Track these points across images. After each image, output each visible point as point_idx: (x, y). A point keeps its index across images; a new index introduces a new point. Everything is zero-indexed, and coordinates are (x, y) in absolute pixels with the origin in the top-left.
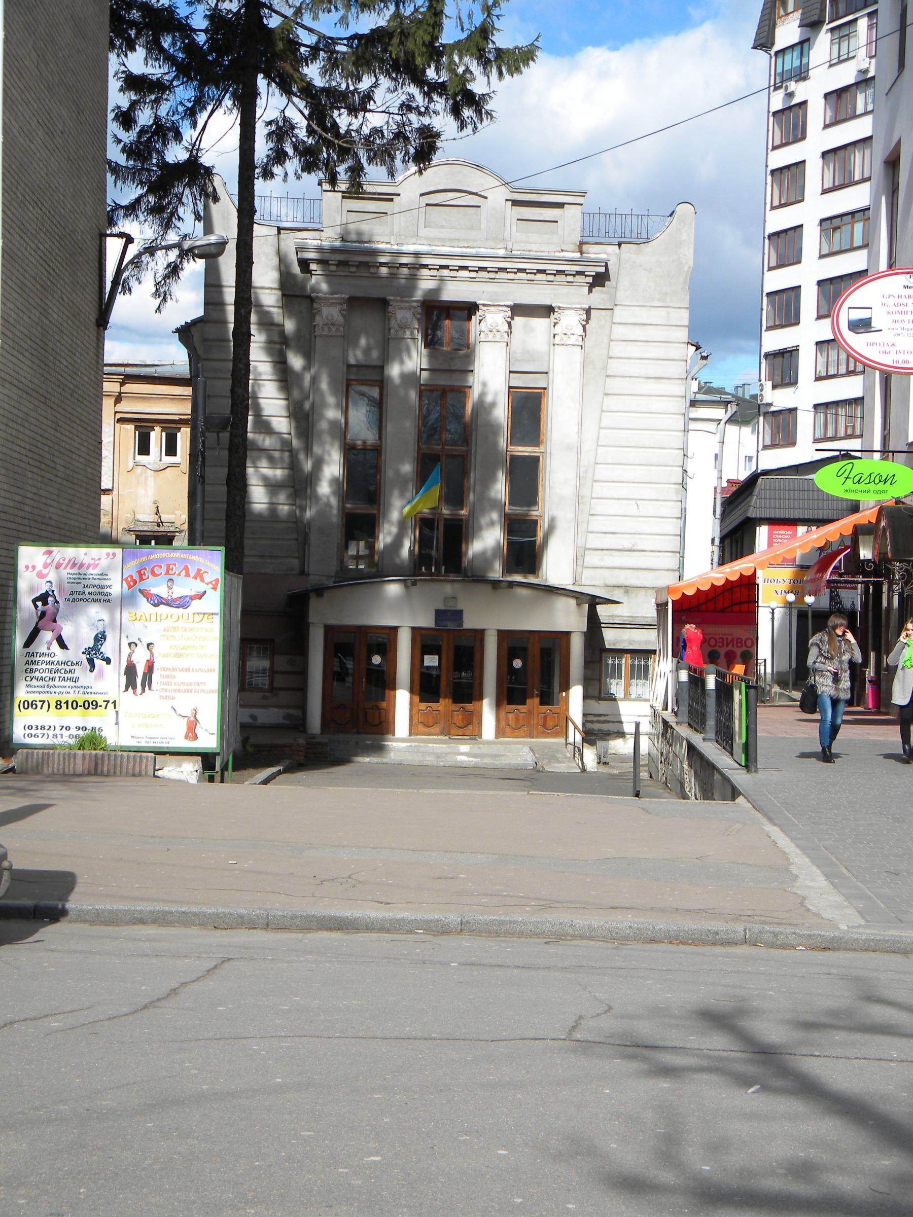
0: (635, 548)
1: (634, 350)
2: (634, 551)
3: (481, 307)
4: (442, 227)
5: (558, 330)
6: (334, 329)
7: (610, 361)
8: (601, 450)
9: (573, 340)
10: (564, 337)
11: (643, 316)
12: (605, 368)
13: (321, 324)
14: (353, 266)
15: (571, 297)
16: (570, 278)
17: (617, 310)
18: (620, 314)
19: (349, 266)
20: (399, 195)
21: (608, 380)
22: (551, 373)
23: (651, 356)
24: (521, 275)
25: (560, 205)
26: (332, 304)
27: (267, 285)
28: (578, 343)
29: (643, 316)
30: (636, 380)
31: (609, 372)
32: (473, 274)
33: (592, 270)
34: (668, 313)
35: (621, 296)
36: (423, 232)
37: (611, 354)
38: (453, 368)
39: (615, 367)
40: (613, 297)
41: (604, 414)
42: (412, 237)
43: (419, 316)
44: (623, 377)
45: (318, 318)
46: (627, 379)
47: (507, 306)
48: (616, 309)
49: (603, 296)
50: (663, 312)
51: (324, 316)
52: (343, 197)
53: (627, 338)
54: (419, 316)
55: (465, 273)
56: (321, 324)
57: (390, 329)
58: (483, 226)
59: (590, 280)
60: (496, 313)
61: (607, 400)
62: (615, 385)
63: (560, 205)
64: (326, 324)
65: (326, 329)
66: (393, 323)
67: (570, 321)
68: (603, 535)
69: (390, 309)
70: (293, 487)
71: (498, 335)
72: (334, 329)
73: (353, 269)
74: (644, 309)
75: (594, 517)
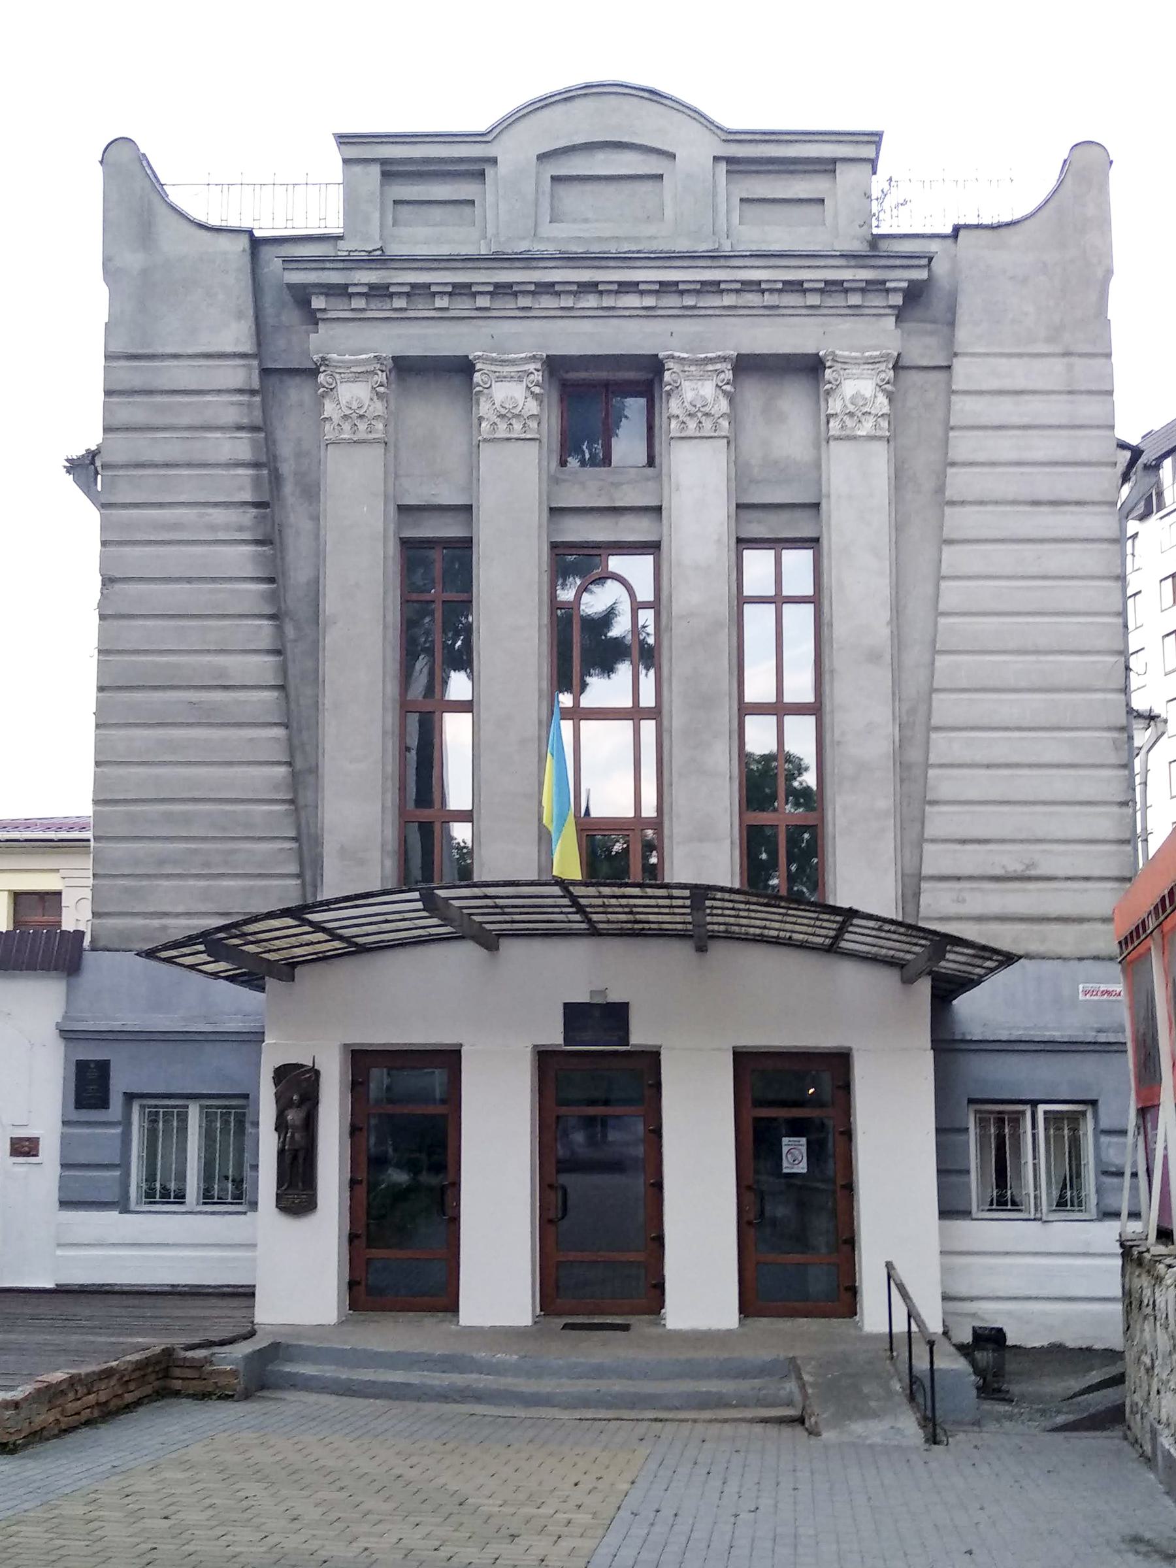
0: (1033, 873)
1: (1004, 447)
2: (1029, 879)
3: (669, 364)
4: (586, 220)
6: (362, 426)
7: (951, 471)
8: (941, 661)
11: (1017, 374)
12: (940, 489)
13: (336, 418)
14: (400, 294)
18: (965, 372)
19: (391, 296)
20: (494, 161)
21: (948, 510)
22: (824, 506)
23: (1039, 455)
24: (753, 299)
25: (828, 167)
26: (358, 377)
27: (229, 349)
28: (879, 433)
29: (1017, 374)
30: (1008, 508)
31: (949, 494)
32: (650, 301)
34: (1070, 368)
35: (962, 334)
36: (547, 229)
37: (953, 455)
38: (617, 504)
39: (959, 482)
40: (950, 340)
41: (944, 584)
42: (524, 238)
43: (537, 390)
44: (982, 503)
46: (990, 508)
48: (959, 365)
49: (932, 341)
50: (1059, 365)
51: (343, 402)
52: (385, 174)
53: (984, 421)
54: (537, 390)
56: (336, 418)
57: (480, 419)
58: (669, 213)
60: (701, 378)
61: (947, 551)
62: (960, 521)
63: (828, 167)
64: (346, 417)
65: (347, 426)
66: (484, 408)
67: (858, 388)
68: (958, 847)
69: (477, 377)
70: (289, 764)
72: (362, 426)
74: (1014, 361)
75: (936, 809)
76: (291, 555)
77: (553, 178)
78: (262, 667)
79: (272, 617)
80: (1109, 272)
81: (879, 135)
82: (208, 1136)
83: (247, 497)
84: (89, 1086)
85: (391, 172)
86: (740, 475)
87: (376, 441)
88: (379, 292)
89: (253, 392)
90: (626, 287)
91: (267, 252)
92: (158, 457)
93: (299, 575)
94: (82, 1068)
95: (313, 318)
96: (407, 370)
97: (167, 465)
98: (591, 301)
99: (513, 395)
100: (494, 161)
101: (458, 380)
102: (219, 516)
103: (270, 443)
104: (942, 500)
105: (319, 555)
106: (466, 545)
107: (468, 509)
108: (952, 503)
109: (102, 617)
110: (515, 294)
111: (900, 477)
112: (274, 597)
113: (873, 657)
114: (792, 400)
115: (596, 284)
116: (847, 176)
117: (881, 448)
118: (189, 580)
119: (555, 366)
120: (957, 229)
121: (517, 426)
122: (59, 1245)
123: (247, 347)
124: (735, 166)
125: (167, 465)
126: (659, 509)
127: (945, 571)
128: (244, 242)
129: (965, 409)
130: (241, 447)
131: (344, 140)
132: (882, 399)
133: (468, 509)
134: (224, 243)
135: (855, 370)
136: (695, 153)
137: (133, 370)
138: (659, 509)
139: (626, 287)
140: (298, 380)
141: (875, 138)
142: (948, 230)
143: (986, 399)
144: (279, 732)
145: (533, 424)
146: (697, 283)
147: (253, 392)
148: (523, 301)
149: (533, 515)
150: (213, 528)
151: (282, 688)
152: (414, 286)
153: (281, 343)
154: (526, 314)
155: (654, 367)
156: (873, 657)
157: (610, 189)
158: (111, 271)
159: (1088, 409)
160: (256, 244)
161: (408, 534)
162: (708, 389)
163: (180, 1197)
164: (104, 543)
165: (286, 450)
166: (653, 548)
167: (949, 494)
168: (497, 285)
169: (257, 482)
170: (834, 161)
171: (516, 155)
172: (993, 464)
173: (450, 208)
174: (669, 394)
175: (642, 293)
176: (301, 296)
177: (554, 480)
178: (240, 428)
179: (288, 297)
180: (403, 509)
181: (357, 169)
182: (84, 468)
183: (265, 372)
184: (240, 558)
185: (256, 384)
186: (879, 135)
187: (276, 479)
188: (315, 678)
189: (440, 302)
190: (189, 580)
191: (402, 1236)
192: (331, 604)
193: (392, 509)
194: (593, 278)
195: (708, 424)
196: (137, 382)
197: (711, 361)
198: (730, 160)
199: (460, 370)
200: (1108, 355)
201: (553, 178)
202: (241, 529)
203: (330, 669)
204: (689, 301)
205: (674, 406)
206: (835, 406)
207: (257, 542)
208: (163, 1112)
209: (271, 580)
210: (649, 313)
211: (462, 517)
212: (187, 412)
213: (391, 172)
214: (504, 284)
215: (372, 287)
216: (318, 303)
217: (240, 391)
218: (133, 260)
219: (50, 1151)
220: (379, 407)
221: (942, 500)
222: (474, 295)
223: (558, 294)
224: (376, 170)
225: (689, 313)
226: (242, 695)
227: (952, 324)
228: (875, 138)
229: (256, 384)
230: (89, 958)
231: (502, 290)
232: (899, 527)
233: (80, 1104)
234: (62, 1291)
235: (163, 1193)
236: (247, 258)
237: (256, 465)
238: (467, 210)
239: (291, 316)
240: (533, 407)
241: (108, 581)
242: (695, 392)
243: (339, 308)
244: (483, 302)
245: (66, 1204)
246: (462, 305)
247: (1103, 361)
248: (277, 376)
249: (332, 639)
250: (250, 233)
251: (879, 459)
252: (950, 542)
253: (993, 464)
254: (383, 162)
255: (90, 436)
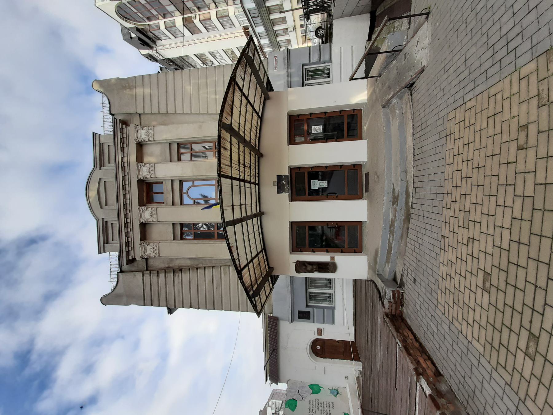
5: (147, 139)
6: (155, 248)
9: (151, 131)
10: (150, 135)
15: (134, 134)
16: (125, 136)
17: (139, 112)
18: (140, 111)
19: (128, 242)
20: (103, 219)
21: (169, 112)
32: (127, 183)
33: (119, 125)
35: (132, 111)
45: (151, 256)
47: (137, 165)
52: (107, 243)
55: (127, 186)
59: (124, 126)
62: (171, 110)
65: (156, 252)
66: (150, 220)
67: (143, 135)
71: (152, 168)
73: (130, 240)
76: (185, 265)
77: (106, 205)
78: (208, 272)
79: (197, 269)
80: (118, 79)
81: (94, 133)
82: (316, 287)
83: (172, 274)
84: (304, 316)
85: (106, 241)
86: (164, 161)
87: (159, 245)
88: (127, 244)
89: (150, 273)
90: (124, 188)
91: (123, 269)
92: (165, 294)
93: (189, 263)
94: (300, 318)
95: (134, 260)
96: (144, 237)
97: (166, 292)
98: (128, 196)
99: (148, 214)
100: (103, 219)
101: (147, 226)
102: (176, 282)
103: (161, 269)
104: (167, 114)
105: (184, 258)
106: (182, 225)
107: (174, 224)
108: (167, 111)
109: (199, 308)
110: (127, 213)
111: (163, 124)
112: (193, 269)
113: (200, 127)
114: (147, 150)
115: (123, 195)
116: (102, 141)
117: (155, 128)
118: (190, 288)
119: (141, 204)
120: (111, 114)
121: (154, 212)
122: (344, 324)
123: (141, 274)
124: (102, 165)
125: (166, 292)
126: (172, 180)
127: (182, 112)
128: (120, 274)
129: (147, 110)
130: (162, 275)
131: (100, 252)
132: (145, 128)
133: (174, 224)
134: (120, 279)
135: (139, 135)
136: (99, 174)
137: (147, 300)
138: (172, 180)
139: (124, 188)
140: (149, 263)
141: (94, 134)
142: (111, 116)
143: (145, 105)
144: (222, 268)
145: (153, 209)
146: (123, 172)
147: (150, 273)
148: (128, 212)
149: (173, 208)
150: (179, 283)
151: (213, 267)
152: (126, 236)
153: (140, 266)
154: (131, 211)
155: (141, 182)
156: (200, 127)
157: (108, 193)
158: (127, 304)
159: (146, 81)
160: (121, 271)
161: (180, 238)
162: (145, 169)
163: (331, 294)
164: (183, 307)
165: (163, 266)
166: (181, 182)
167: (165, 112)
168: (125, 218)
169: (170, 272)
170: (100, 143)
171: (101, 214)
172: (159, 102)
173: (114, 229)
174: (146, 178)
175: (125, 185)
176: (130, 262)
177: (167, 204)
178: (158, 276)
179: (132, 265)
180: (174, 239)
181: (106, 249)
182: (171, 311)
183: (147, 270)
184: (185, 276)
185: (149, 272)
186: (94, 133)
187: (169, 268)
188: (210, 260)
189: (129, 230)
190: (190, 288)
191: (345, 237)
192: (194, 256)
193: (174, 241)
194: (123, 195)
195: (152, 168)
196: (149, 298)
197: (138, 168)
198: (101, 167)
199: (144, 226)
200: (135, 77)
201: (106, 205)
202: (179, 276)
203: (208, 256)
204: (126, 174)
205: (148, 176)
206: (147, 140)
207: (181, 273)
208: (311, 297)
209: (189, 269)
210: (130, 183)
211: (175, 226)
212: (155, 288)
213: (106, 241)
214: (125, 215)
215: (126, 246)
216: (131, 258)
217: (150, 276)
218: (125, 299)
219: (321, 326)
220: (151, 244)
221: (167, 114)
222: (127, 223)
223: (126, 204)
224: (106, 245)
225: (129, 174)
226: (214, 277)
227: (131, 114)
228: (94, 134)
229: (149, 272)
230: (275, 314)
231: (126, 216)
232: (173, 123)
233: (309, 318)
234: (355, 325)
235: (330, 298)
236: (123, 273)
237: (165, 272)
238: (114, 225)
239: (135, 264)
240: (150, 209)
241: (191, 307)
242: (145, 173)
243: (132, 253)
244: (129, 221)
245: (333, 323)
246: (130, 225)
247: (137, 79)
248: (147, 267)
249: (201, 256)
250: (118, 273)
251: (158, 129)
252: (175, 111)
253: (159, 102)
254: (104, 243)
255: (165, 310)
